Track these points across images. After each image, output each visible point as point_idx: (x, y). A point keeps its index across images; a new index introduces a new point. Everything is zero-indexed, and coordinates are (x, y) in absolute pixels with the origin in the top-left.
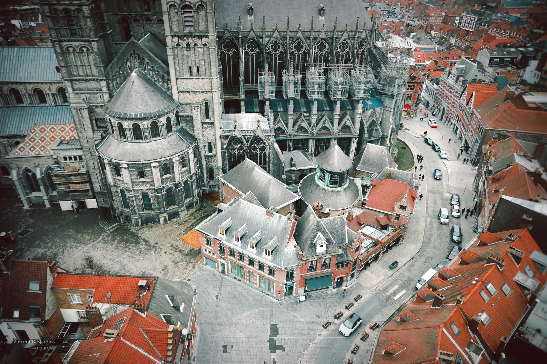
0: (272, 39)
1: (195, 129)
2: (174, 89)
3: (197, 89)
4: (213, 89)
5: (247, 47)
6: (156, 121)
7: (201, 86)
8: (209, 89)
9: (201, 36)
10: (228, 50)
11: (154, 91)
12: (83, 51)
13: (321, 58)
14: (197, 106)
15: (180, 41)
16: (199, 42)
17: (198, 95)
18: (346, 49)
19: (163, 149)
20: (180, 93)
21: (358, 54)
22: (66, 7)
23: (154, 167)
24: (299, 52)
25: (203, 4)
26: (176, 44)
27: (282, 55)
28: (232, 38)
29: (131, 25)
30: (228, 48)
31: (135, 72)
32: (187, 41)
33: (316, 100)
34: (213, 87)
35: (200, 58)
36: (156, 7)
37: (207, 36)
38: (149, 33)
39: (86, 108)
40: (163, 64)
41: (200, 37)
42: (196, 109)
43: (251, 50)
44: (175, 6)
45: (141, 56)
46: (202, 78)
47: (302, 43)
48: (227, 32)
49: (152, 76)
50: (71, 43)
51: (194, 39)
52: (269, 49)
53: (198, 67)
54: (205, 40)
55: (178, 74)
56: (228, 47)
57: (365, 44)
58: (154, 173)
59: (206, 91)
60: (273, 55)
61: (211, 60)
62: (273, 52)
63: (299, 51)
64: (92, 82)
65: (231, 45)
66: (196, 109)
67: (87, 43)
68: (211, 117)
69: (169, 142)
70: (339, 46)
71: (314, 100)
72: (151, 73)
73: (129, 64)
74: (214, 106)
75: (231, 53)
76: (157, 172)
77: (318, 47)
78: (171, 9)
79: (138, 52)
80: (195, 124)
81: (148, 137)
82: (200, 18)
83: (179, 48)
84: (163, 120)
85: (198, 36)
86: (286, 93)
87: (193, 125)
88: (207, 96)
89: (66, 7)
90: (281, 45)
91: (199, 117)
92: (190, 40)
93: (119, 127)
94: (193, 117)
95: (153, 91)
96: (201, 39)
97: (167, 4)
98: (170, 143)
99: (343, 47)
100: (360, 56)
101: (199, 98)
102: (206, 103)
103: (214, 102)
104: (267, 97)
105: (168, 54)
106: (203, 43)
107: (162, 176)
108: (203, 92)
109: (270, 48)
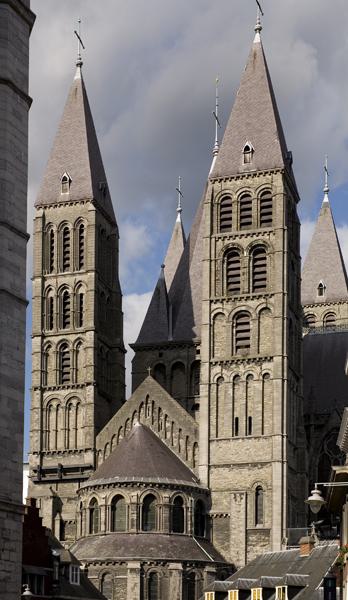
1: (232, 542)
2: (202, 459)
3: (245, 459)
6: (155, 494)
8: (267, 458)
17: (245, 471)
19: (156, 546)
22: (64, 337)
23: (132, 570)
42: (239, 499)
45: (157, 405)
50: (58, 392)
58: (130, 585)
66: (239, 499)
67: (79, 391)
69: (172, 542)
80: (233, 532)
87: (228, 537)
89: (64, 337)
101: (245, 479)
102: (259, 489)
103: (274, 484)
108: (255, 465)
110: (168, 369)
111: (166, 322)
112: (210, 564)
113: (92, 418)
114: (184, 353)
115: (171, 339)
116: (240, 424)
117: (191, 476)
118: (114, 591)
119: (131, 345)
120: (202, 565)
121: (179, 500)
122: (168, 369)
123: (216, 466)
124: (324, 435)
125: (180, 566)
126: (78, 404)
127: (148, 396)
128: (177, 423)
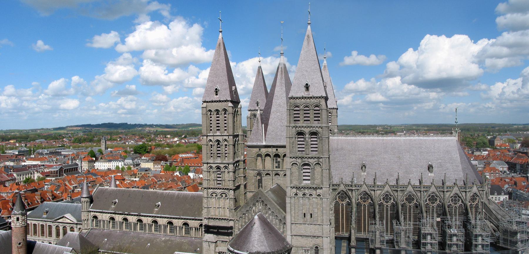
0: (383, 192)
2: (289, 233)
4: (324, 235)
5: (359, 199)
7: (313, 231)
8: (320, 234)
9: (316, 188)
10: (343, 201)
11: (271, 233)
12: (222, 196)
13: (433, 210)
14: (308, 250)
15: (297, 191)
16: (314, 192)
17: (310, 239)
18: (458, 202)
20: (293, 237)
21: (471, 208)
22: (218, 165)
24: (411, 204)
25: (319, 162)
26: (294, 194)
27: (395, 206)
28: (346, 190)
29: (263, 178)
30: (342, 198)
31: (258, 215)
32: (304, 191)
33: (430, 252)
34: (324, 233)
35: (314, 206)
36: (284, 164)
37: (322, 188)
38: (276, 185)
39: (214, 242)
40: (281, 210)
41: (315, 189)
42: (307, 252)
43: (363, 201)
44: (296, 164)
45: (265, 203)
46: (314, 224)
47: (413, 196)
48: (342, 185)
49: (272, 221)
50: (216, 190)
51: (309, 190)
52: (380, 200)
53: (311, 214)
54: (319, 191)
55: (293, 219)
56: (342, 197)
57: (478, 198)
59: (317, 237)
60: (385, 206)
61: (324, 208)
62: (385, 203)
63: (410, 203)
64: (223, 221)
65: (345, 196)
67: (226, 191)
70: (450, 199)
71: (428, 251)
72: (271, 217)
73: (254, 208)
75: (344, 203)
77: (429, 200)
78: (293, 167)
82: (316, 174)
83: (296, 198)
85: (313, 188)
86: (397, 242)
88: (318, 241)
89: (218, 165)
90: (392, 198)
92: (306, 191)
95: (270, 233)
96: (316, 190)
99: (455, 200)
100: (474, 210)
102: (317, 247)
103: (324, 247)
104: (378, 245)
105: (287, 202)
106: (317, 194)
108: (315, 237)
109: (382, 199)
110: (263, 156)
111: (262, 134)
113: (233, 205)
114: (270, 150)
117: (283, 240)
122: (263, 156)
124: (337, 193)
126: (226, 196)
127: (260, 198)
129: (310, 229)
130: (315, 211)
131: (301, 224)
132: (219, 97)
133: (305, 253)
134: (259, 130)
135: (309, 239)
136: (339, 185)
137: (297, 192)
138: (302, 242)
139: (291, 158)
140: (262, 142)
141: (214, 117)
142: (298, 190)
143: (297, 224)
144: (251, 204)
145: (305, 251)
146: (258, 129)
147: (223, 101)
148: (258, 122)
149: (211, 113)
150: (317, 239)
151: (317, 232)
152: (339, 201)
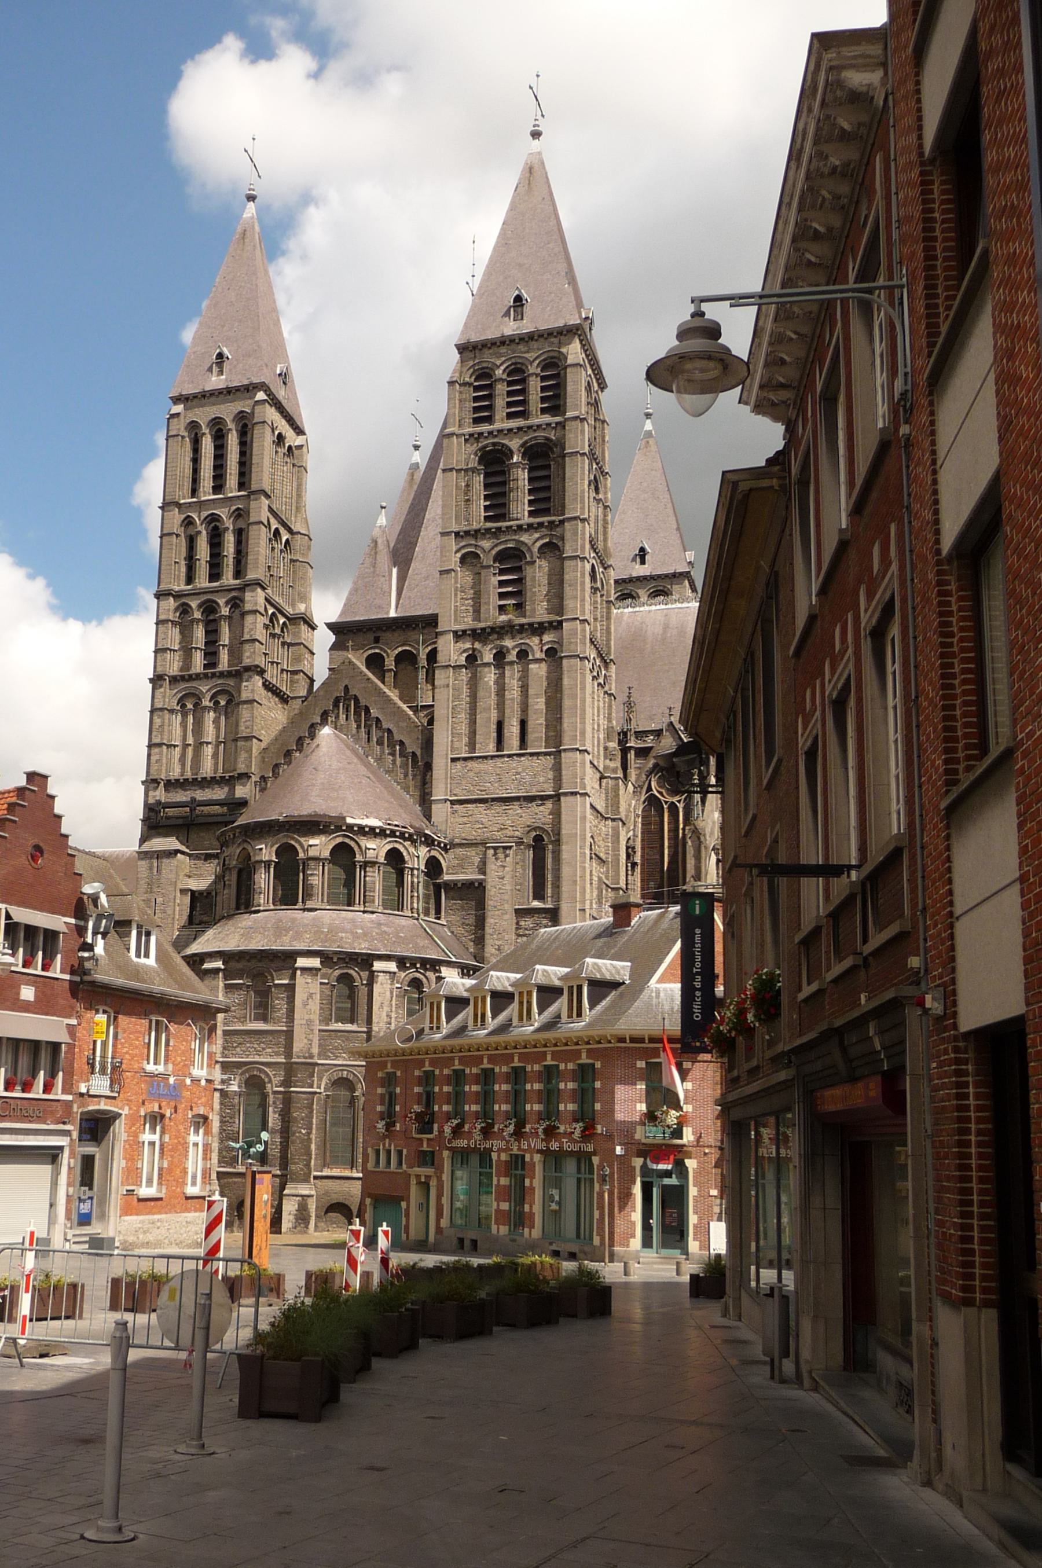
2: (439, 792)
6: (352, 844)
15: (477, 645)
17: (515, 808)
19: (352, 933)
23: (304, 970)
26: (465, 655)
32: (498, 642)
41: (538, 629)
42: (501, 855)
45: (363, 702)
46: (532, 754)
55: (456, 745)
58: (300, 996)
66: (501, 855)
68: (549, 891)
74: (564, 847)
76: (311, 996)
79: (353, 692)
81: (315, 891)
84: (376, 849)
91: (508, 887)
92: (508, 643)
93: (240, 872)
94: (488, 887)
97: (457, 551)
98: (385, 928)
103: (563, 832)
106: (545, 648)
107: (327, 1020)
108: (530, 799)
112: (449, 964)
115: (392, 614)
116: (506, 733)
118: (273, 1007)
119: (330, 626)
120: (433, 965)
121: (395, 858)
123: (461, 802)
125: (392, 966)
127: (346, 687)
128: (395, 731)
129: (518, 773)
130: (536, 707)
131: (485, 757)
132: (226, 380)
133: (496, 859)
134: (378, 575)
135: (510, 812)
136: (658, 733)
137: (474, 650)
138: (487, 824)
139: (457, 534)
140: (388, 612)
141: (207, 445)
142: (480, 642)
143: (471, 758)
144: (314, 714)
145: (495, 854)
146: (374, 572)
147: (237, 389)
148: (376, 553)
149: (196, 434)
150: (541, 808)
151: (542, 779)
152: (661, 793)
